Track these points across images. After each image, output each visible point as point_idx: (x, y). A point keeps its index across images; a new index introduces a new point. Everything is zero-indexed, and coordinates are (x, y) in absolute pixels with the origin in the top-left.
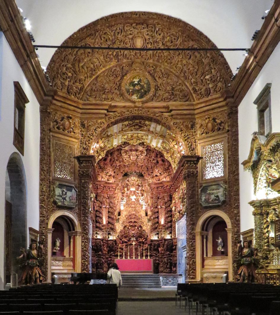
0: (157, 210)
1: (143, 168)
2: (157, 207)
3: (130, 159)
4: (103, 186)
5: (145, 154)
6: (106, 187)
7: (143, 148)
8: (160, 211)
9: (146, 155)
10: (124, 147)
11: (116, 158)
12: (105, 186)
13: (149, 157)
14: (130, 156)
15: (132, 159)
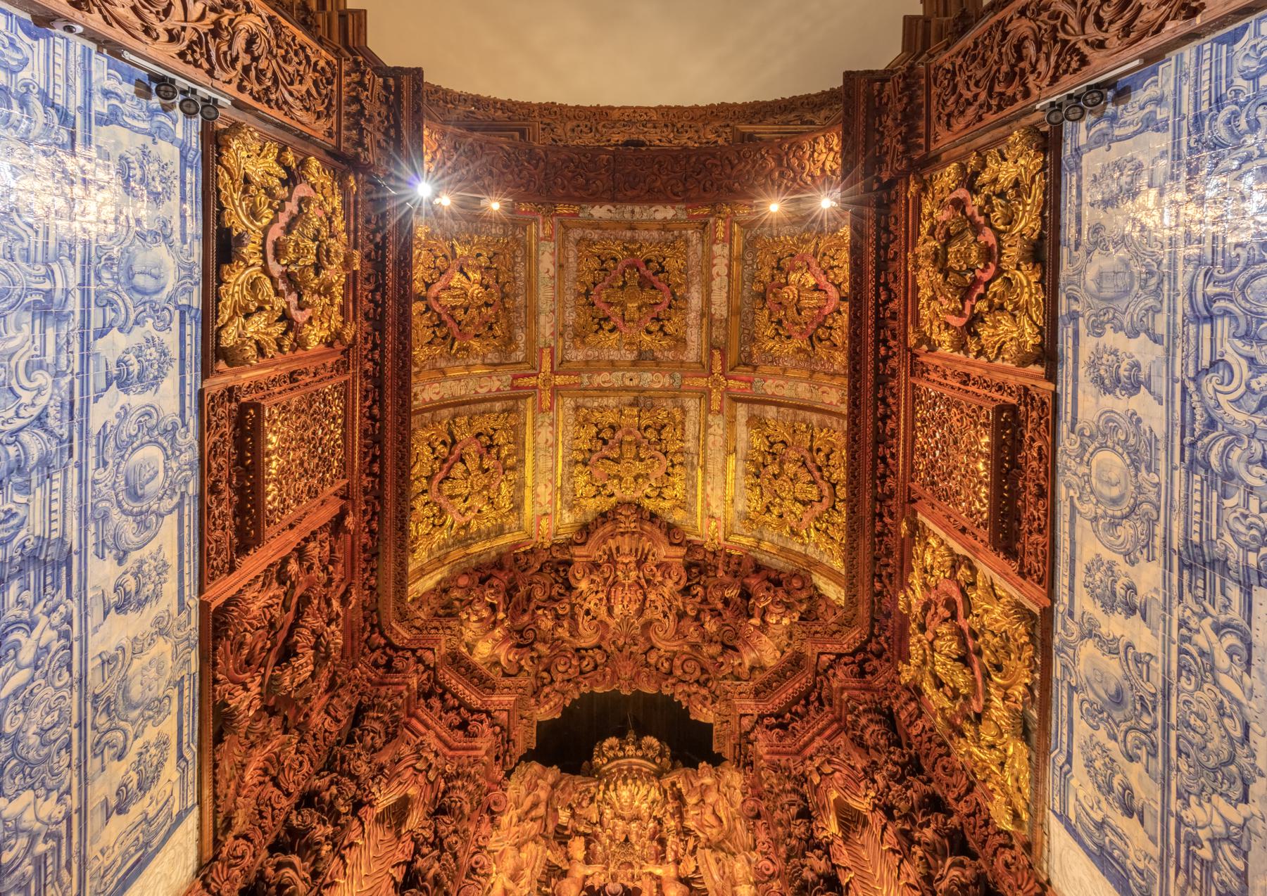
0: (821, 865)
1: (677, 662)
2: (812, 843)
3: (610, 610)
4: (428, 656)
5: (683, 582)
6: (448, 696)
7: (672, 544)
8: (844, 859)
9: (686, 591)
10: (583, 544)
11: (539, 594)
12: (446, 690)
13: (705, 601)
14: (609, 593)
15: (618, 610)
